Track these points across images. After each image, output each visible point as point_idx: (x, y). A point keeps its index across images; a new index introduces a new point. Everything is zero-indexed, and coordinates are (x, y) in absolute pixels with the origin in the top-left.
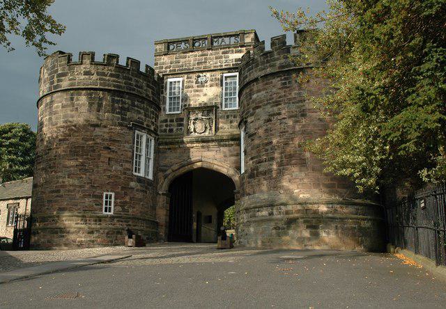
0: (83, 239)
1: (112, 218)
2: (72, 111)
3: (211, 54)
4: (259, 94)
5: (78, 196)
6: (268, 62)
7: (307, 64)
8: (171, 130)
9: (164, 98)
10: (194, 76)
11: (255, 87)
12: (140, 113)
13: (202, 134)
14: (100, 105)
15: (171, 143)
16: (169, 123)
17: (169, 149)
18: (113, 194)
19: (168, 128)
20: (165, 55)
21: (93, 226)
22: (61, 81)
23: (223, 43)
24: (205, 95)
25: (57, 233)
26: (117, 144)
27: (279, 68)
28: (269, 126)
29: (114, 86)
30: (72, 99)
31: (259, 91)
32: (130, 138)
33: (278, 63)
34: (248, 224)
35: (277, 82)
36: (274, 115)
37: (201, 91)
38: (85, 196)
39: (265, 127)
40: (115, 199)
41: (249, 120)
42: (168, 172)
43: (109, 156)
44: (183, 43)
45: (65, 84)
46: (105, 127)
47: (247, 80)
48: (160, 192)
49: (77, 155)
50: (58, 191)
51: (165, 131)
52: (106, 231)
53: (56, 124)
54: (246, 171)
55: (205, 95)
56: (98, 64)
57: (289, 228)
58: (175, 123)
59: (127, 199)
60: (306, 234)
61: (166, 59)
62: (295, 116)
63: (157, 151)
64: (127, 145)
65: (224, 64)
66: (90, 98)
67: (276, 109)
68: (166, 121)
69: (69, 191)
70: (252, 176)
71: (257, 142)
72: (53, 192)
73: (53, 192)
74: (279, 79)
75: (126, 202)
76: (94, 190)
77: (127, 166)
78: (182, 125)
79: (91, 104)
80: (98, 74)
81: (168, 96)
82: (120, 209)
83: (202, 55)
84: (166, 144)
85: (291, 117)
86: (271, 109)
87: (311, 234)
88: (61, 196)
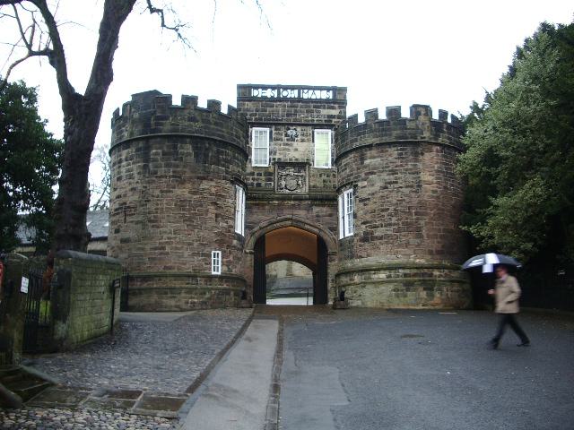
0: (196, 300)
1: (221, 278)
2: (175, 160)
3: (301, 107)
4: (372, 160)
5: (186, 254)
6: (383, 130)
7: (422, 138)
8: (259, 185)
9: (250, 148)
10: (283, 128)
11: (368, 153)
12: (238, 166)
13: (294, 192)
14: (206, 156)
15: (259, 199)
16: (256, 177)
17: (258, 205)
18: (220, 252)
19: (255, 182)
20: (250, 101)
21: (205, 286)
22: (162, 125)
23: (314, 97)
24: (296, 150)
25: (166, 293)
26: (223, 199)
27: (396, 138)
28: (386, 193)
29: (219, 135)
30: (175, 147)
31: (374, 157)
32: (232, 193)
33: (395, 133)
34: (363, 285)
35: (393, 152)
36: (390, 183)
37: (291, 145)
38: (194, 254)
39: (381, 194)
40: (223, 258)
41: (360, 184)
42: (255, 229)
43: (215, 211)
44: (269, 90)
45: (166, 127)
46: (211, 180)
47: (357, 144)
48: (248, 251)
49: (184, 210)
50: (164, 248)
51: (252, 184)
52: (217, 292)
53: (156, 173)
54: (355, 235)
55: (296, 150)
56: (202, 110)
57: (408, 290)
58: (263, 177)
59: (231, 258)
60: (423, 294)
61: (249, 105)
62: (412, 187)
63: (248, 207)
64: (230, 201)
65: (315, 119)
66: (195, 148)
67: (392, 178)
68: (253, 174)
69: (176, 248)
70: (365, 239)
71: (371, 206)
72: (156, 249)
73: (156, 249)
74: (393, 149)
75: (229, 262)
76: (203, 248)
77: (231, 222)
78: (270, 180)
79: (197, 155)
80: (203, 121)
81: (253, 147)
82: (225, 268)
83: (291, 107)
84: (254, 199)
85: (407, 187)
86: (387, 178)
87: (427, 295)
88: (167, 253)
